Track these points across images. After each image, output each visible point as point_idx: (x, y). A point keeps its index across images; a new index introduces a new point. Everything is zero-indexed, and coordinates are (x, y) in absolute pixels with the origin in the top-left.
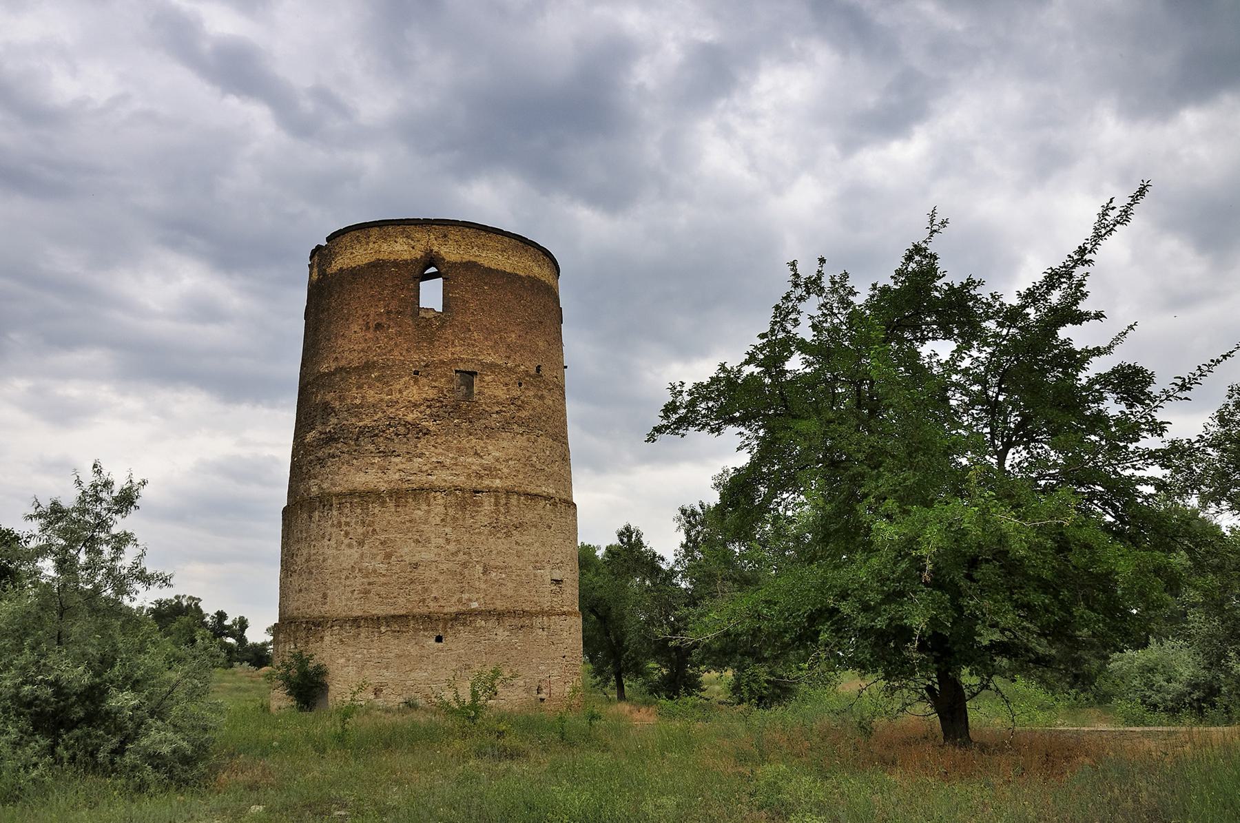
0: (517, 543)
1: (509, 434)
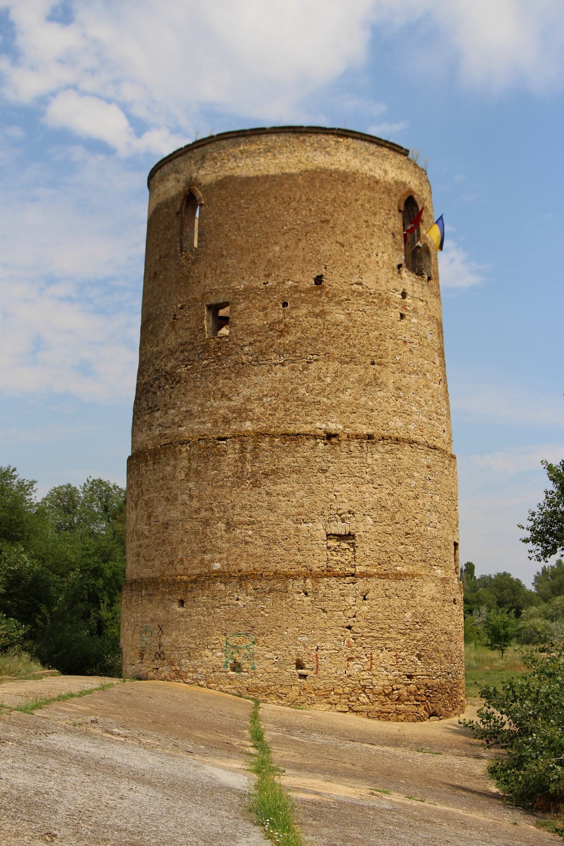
0: (268, 494)
1: (264, 366)
